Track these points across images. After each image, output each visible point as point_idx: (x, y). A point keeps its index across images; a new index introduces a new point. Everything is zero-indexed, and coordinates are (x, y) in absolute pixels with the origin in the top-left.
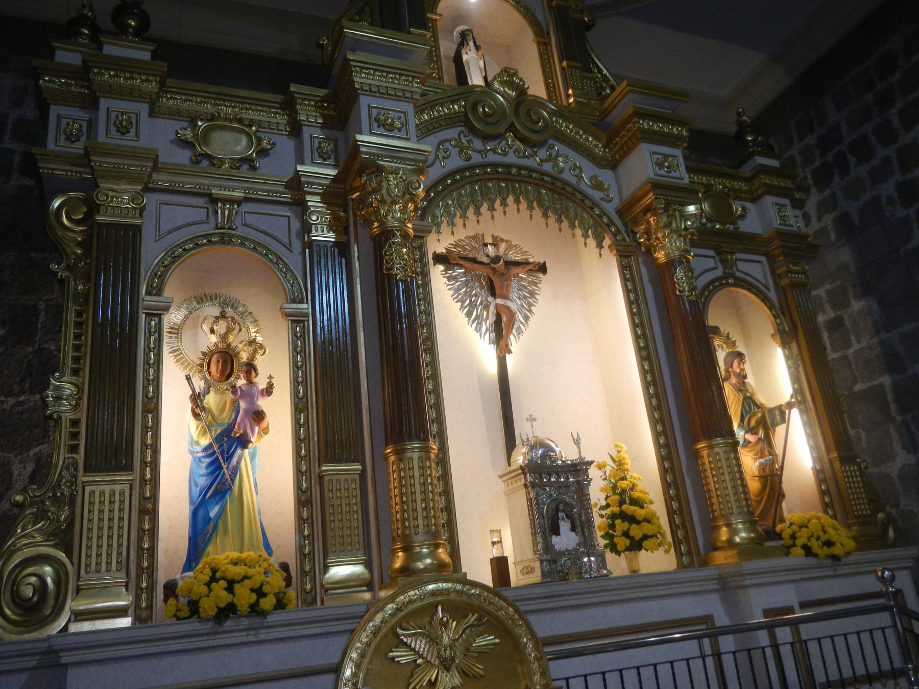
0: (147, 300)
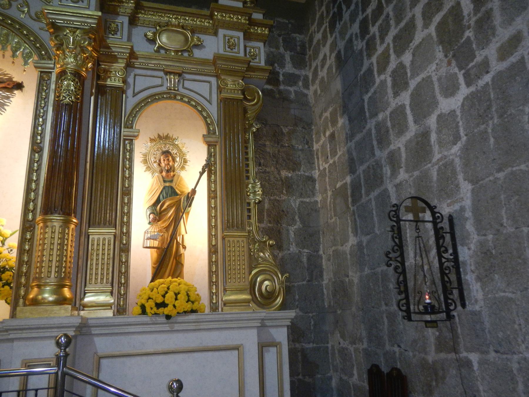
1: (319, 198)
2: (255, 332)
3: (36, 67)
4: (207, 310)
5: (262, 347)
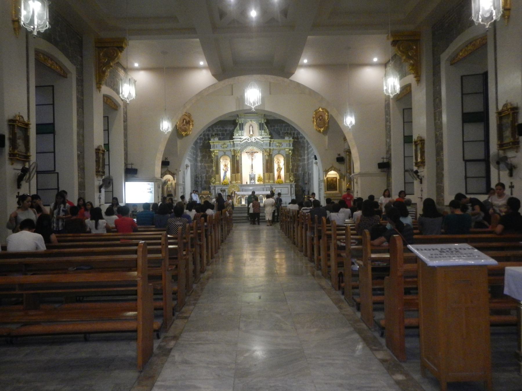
1: (306, 162)
2: (290, 186)
5: (291, 187)
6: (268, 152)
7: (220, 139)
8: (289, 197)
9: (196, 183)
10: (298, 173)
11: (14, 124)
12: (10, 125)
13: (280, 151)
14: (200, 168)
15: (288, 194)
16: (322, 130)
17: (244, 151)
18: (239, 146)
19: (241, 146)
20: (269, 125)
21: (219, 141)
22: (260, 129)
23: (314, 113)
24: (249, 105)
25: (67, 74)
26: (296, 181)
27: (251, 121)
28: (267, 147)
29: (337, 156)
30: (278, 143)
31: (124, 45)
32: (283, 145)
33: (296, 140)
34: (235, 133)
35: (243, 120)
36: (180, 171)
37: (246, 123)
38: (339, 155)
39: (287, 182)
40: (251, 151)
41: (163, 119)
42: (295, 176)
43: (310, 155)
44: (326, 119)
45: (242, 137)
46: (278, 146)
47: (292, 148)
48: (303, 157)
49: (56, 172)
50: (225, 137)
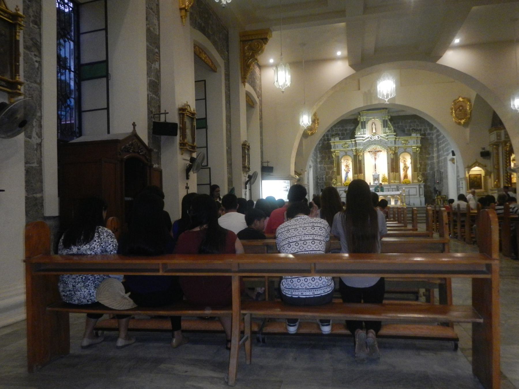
0: (340, 162)
1: (435, 161)
3: (387, 151)
4: (411, 183)
5: (419, 188)
6: (393, 150)
7: (340, 139)
8: (416, 198)
9: (318, 185)
10: (426, 173)
11: (184, 112)
12: (180, 114)
13: (406, 148)
14: (320, 170)
15: (416, 195)
16: (463, 121)
17: (367, 150)
18: (361, 145)
19: (363, 145)
20: (392, 122)
21: (341, 141)
22: (384, 127)
23: (453, 103)
24: (381, 98)
25: (216, 69)
26: (425, 181)
27: (373, 118)
28: (393, 145)
29: (481, 150)
30: (404, 140)
31: (268, 37)
32: (409, 142)
33: (423, 137)
34: (357, 132)
35: (365, 117)
36: (306, 171)
37: (368, 120)
38: (484, 149)
39: (414, 182)
40: (374, 150)
41: (302, 112)
42: (423, 175)
43: (442, 152)
44: (468, 109)
45: (364, 136)
46: (403, 144)
47: (419, 145)
48: (431, 154)
49: (209, 166)
50: (344, 136)
